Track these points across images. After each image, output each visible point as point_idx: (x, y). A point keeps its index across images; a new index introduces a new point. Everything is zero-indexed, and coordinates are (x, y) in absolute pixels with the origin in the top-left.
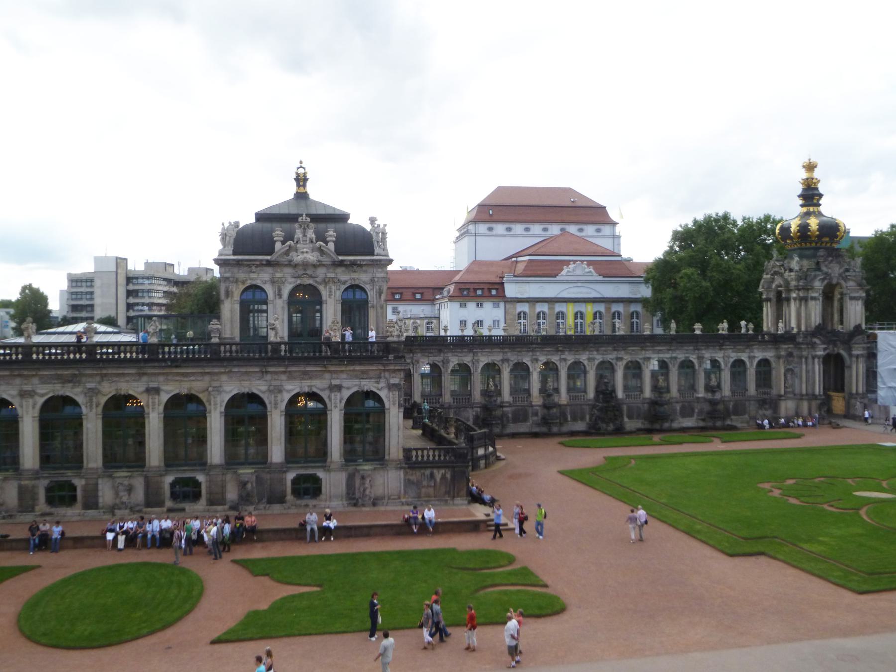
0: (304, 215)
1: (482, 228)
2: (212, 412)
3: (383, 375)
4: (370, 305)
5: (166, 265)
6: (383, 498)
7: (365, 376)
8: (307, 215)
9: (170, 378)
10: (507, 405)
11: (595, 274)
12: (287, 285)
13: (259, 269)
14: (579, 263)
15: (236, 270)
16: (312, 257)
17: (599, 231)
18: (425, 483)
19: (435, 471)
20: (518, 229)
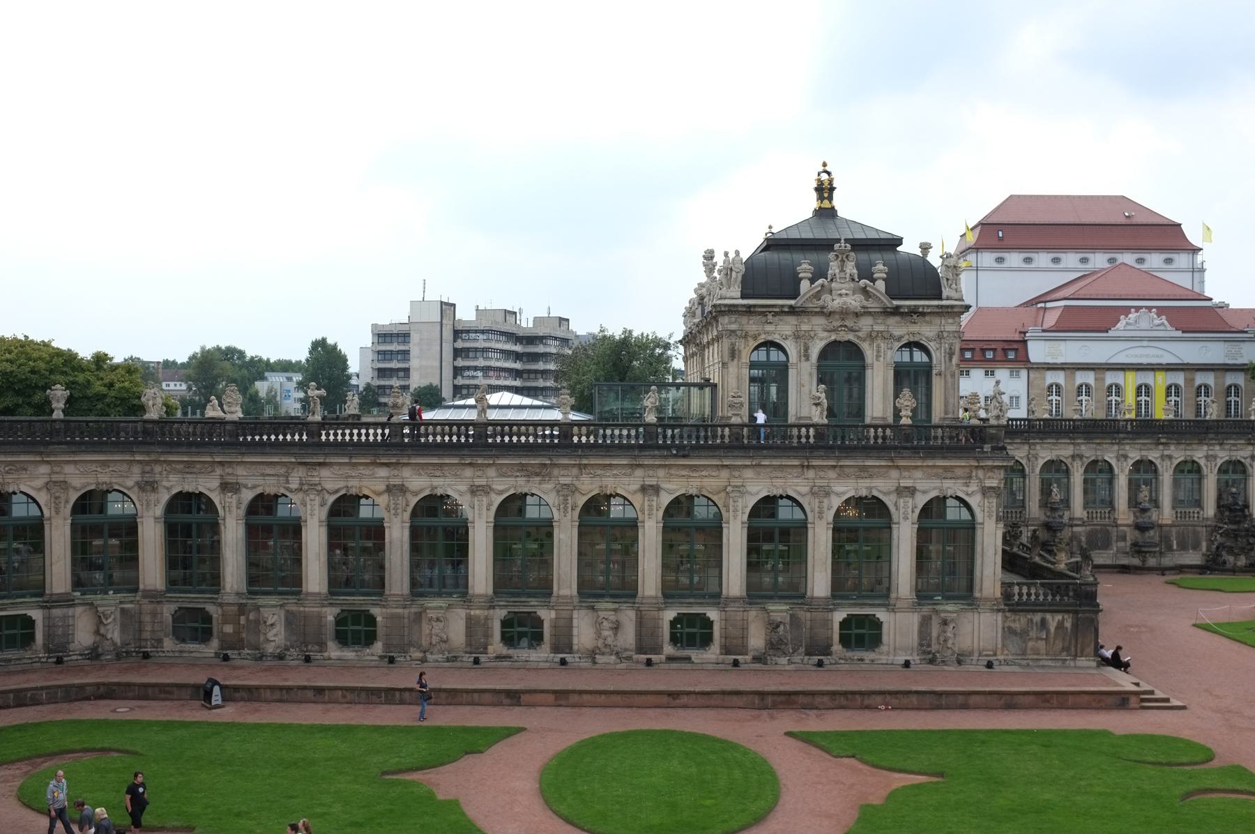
0: (842, 241)
1: (987, 258)
2: (731, 518)
3: (974, 474)
4: (934, 372)
5: (507, 312)
6: (971, 654)
7: (949, 475)
8: (847, 240)
9: (673, 472)
10: (1080, 523)
11: (1169, 328)
12: (818, 341)
13: (777, 318)
14: (1144, 310)
15: (744, 320)
16: (855, 302)
17: (1169, 261)
18: (1033, 634)
19: (1048, 616)
20: (1042, 259)
